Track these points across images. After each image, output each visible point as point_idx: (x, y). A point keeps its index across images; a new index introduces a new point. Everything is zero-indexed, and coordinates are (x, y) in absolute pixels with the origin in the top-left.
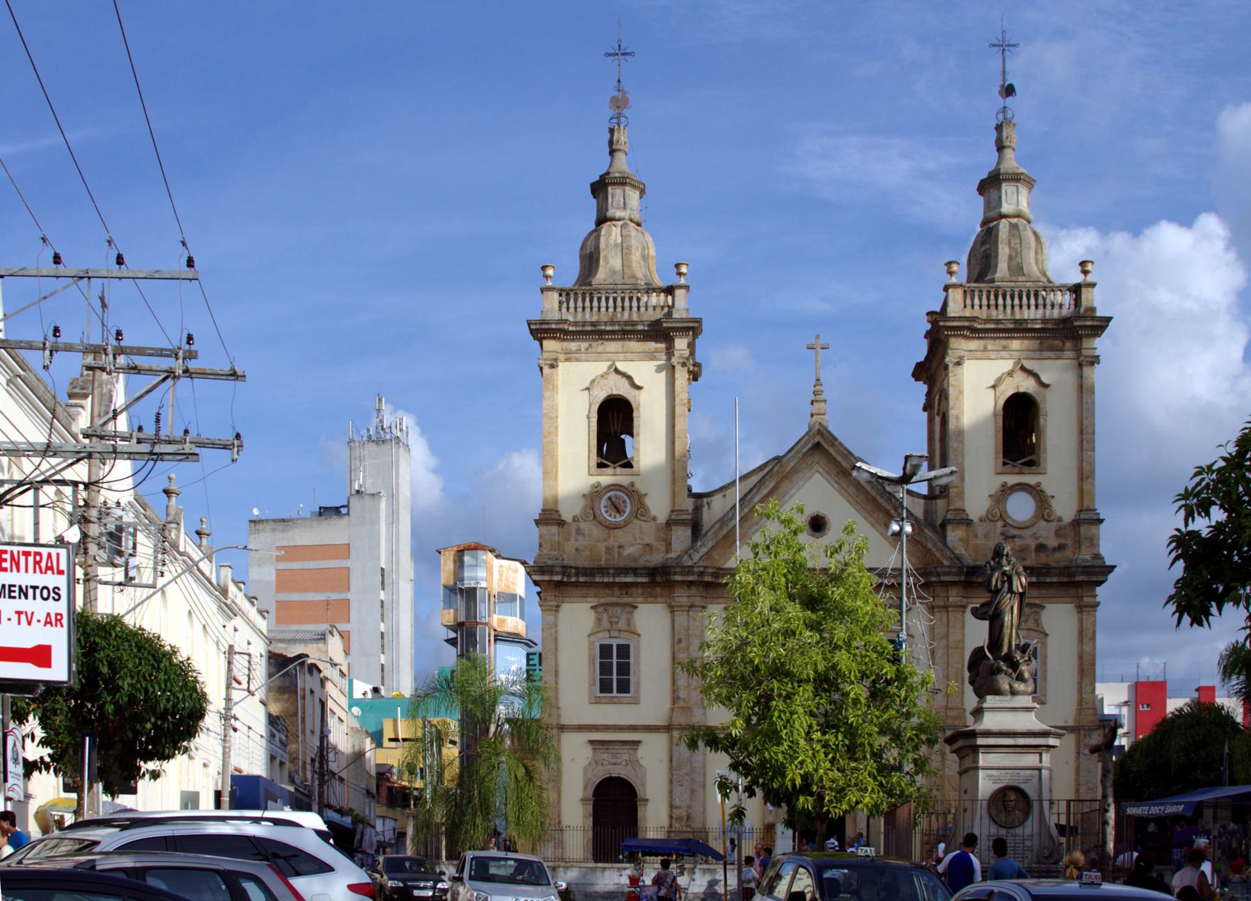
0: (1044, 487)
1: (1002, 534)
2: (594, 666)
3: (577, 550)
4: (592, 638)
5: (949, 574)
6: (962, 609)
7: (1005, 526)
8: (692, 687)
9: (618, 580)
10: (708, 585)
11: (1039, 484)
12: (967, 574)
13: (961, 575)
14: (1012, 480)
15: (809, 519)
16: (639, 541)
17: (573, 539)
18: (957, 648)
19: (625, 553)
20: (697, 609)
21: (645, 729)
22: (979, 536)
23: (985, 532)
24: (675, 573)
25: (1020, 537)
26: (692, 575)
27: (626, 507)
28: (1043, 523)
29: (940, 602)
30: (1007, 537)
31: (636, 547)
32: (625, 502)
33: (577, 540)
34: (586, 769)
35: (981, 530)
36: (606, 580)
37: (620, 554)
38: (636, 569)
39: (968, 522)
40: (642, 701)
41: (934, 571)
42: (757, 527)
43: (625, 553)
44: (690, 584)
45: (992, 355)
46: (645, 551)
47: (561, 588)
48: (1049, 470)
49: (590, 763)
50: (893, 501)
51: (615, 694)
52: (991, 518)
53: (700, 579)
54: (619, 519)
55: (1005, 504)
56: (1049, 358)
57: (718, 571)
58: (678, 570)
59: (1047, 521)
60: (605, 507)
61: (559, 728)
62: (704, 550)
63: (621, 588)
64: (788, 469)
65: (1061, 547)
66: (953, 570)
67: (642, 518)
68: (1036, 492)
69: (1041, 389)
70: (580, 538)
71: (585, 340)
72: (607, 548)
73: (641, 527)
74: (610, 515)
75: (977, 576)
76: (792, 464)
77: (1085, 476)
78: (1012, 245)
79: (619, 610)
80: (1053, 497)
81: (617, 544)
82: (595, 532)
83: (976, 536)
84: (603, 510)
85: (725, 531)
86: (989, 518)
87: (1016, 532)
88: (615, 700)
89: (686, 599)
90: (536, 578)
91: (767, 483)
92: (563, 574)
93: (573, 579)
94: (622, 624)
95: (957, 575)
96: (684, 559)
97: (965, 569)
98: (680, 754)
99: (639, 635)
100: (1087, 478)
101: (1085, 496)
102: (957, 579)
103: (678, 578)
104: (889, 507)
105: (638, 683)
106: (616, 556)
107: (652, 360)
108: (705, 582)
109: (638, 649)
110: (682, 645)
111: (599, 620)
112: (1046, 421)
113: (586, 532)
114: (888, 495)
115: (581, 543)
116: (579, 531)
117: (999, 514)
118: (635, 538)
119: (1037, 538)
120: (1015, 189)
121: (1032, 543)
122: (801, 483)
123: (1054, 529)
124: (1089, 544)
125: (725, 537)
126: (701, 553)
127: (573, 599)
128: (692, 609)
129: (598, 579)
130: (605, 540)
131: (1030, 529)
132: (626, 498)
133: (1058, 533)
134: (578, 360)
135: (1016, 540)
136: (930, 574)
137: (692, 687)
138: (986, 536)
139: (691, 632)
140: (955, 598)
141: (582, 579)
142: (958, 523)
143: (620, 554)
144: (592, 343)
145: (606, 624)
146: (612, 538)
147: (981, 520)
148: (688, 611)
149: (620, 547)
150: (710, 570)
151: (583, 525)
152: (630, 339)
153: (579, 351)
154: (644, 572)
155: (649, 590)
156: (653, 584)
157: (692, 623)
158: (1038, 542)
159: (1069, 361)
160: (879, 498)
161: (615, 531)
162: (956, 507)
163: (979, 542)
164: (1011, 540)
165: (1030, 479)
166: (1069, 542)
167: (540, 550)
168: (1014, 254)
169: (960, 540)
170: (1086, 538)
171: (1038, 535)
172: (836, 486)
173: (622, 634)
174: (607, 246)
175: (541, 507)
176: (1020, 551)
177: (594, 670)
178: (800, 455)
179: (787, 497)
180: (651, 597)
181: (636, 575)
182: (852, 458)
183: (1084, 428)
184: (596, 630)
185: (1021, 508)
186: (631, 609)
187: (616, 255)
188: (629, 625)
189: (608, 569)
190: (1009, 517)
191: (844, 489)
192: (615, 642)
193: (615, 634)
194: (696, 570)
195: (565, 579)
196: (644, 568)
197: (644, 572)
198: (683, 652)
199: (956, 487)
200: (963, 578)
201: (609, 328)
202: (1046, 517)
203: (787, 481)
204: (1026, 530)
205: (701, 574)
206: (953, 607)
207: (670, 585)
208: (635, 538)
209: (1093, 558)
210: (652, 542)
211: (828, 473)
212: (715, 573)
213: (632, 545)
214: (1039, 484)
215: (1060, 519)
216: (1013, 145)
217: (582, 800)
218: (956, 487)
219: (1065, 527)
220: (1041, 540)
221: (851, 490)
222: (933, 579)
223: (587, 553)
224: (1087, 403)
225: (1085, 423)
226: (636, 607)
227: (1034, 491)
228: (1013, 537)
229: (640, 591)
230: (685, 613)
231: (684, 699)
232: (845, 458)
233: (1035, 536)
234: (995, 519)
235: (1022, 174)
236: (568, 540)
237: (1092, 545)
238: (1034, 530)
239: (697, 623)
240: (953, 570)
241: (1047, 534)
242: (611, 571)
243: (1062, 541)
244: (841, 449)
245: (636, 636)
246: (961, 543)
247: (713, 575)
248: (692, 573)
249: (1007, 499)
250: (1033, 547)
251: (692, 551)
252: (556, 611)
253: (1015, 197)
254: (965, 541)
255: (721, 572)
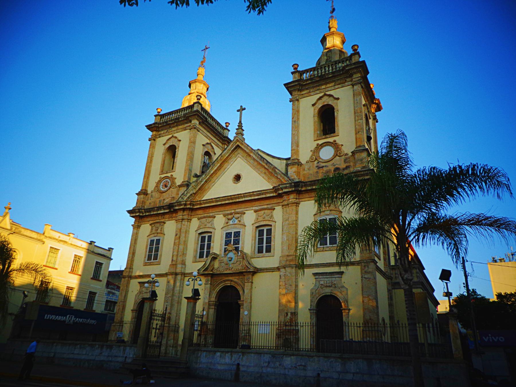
0: (337, 142)
1: (317, 167)
2: (147, 249)
3: (150, 203)
4: (148, 237)
5: (286, 188)
6: (296, 205)
7: (318, 163)
8: (179, 255)
9: (159, 212)
10: (192, 210)
11: (335, 141)
12: (295, 186)
13: (292, 188)
14: (320, 142)
15: (234, 176)
16: (170, 196)
17: (149, 199)
18: (293, 224)
19: (165, 202)
20: (185, 220)
21: (159, 276)
22: (306, 169)
23: (308, 167)
24: (176, 206)
25: (326, 166)
26: (182, 205)
27: (168, 184)
28: (337, 158)
29: (285, 203)
30: (319, 168)
31: (169, 199)
32: (169, 182)
33: (150, 200)
34: (136, 296)
35: (306, 167)
36: (155, 213)
37: (163, 202)
38: (163, 206)
39: (299, 164)
40: (162, 263)
41: (279, 188)
42: (214, 184)
43: (165, 202)
44: (184, 210)
45: (312, 94)
46: (172, 200)
47: (143, 219)
48: (340, 134)
49: (138, 293)
50: (265, 161)
51: (152, 261)
52: (311, 160)
53: (185, 207)
54: (166, 189)
55: (319, 153)
56: (339, 88)
57: (192, 202)
58: (176, 204)
59: (339, 156)
60: (162, 185)
61: (128, 277)
62: (189, 195)
63: (162, 216)
64: (225, 157)
65: (347, 167)
66: (287, 185)
67: (173, 187)
68: (334, 145)
69: (335, 101)
70: (152, 199)
71: (165, 129)
72: (160, 201)
73: (172, 191)
74: (163, 188)
75: (302, 187)
76: (227, 155)
77: (357, 132)
78: (328, 55)
79: (158, 225)
80: (342, 145)
81: (163, 199)
82: (156, 195)
83: (304, 170)
84: (161, 187)
85: (199, 187)
86: (311, 161)
87: (324, 164)
88: (152, 264)
89: (181, 217)
90: (132, 215)
91: (216, 164)
92: (139, 212)
93: (144, 214)
94: (159, 231)
95: (290, 188)
96: (180, 200)
97: (293, 184)
98: (169, 287)
99: (164, 235)
100: (358, 132)
101: (358, 141)
102: (290, 190)
103: (177, 208)
104: (264, 164)
105: (161, 255)
106: (162, 203)
107: (185, 130)
108: (189, 208)
109: (163, 241)
110: (178, 236)
111: (152, 229)
112: (338, 113)
113: (154, 196)
114: (263, 159)
115: (152, 200)
116: (152, 196)
117: (315, 158)
118: (169, 195)
119: (334, 166)
120: (332, 38)
121: (332, 168)
122: (232, 163)
123: (343, 159)
124: (360, 163)
125: (199, 189)
126: (187, 197)
127: (146, 223)
128: (183, 221)
129: (152, 213)
130: (159, 198)
131: (331, 162)
132: (169, 181)
133: (345, 161)
134: (163, 136)
135: (324, 168)
136: (278, 189)
137: (179, 255)
138: (309, 169)
139: (182, 231)
140: (292, 200)
141: (147, 214)
142: (293, 165)
143: (163, 202)
144: (168, 130)
145: (154, 231)
146: (162, 197)
147: (307, 162)
148: (182, 222)
149: (164, 200)
150: (188, 203)
151: (153, 194)
152: (179, 125)
153: (164, 133)
154: (166, 207)
155: (171, 215)
156: (170, 212)
157: (183, 227)
158: (335, 167)
159: (349, 86)
160: (260, 162)
161: (163, 194)
162: (294, 158)
163: (305, 172)
164: (321, 168)
165: (331, 140)
166: (352, 164)
167: (136, 205)
168: (328, 58)
169: (294, 172)
170: (359, 160)
171: (335, 164)
172: (245, 161)
173: (159, 235)
174: (184, 101)
175: (141, 189)
176: (326, 173)
177: (147, 251)
178: (230, 151)
179: (226, 170)
180: (170, 219)
181: (164, 209)
182: (249, 147)
183: (356, 111)
184: (150, 234)
185: (327, 153)
186: (163, 224)
187: (187, 102)
188: (161, 231)
189: (154, 208)
190: (320, 158)
191: (248, 161)
192: (155, 238)
193: (156, 235)
194: (182, 203)
195: (141, 214)
196: (166, 206)
197: (166, 207)
198: (177, 240)
199: (294, 150)
200: (293, 189)
201: (171, 122)
202: (338, 154)
203: (227, 163)
204: (329, 163)
205: (185, 205)
206: (291, 204)
207: (176, 211)
208: (169, 195)
209: (361, 169)
210: (175, 196)
211: (243, 156)
212: (190, 203)
213: (168, 198)
214: (335, 141)
215: (346, 154)
216: (335, 26)
217: (132, 310)
218: (294, 150)
219: (349, 158)
220: (337, 166)
221: (252, 161)
222: (280, 192)
223: (153, 204)
224: (357, 100)
225: (356, 109)
226: (165, 223)
227: (333, 145)
228: (323, 167)
229: (168, 216)
230: (181, 222)
231: (175, 261)
232: (247, 148)
233: (333, 165)
234: (313, 160)
235: (334, 31)
236: (148, 200)
237: (362, 163)
238: (333, 161)
239: (185, 227)
240: (287, 185)
241: (340, 163)
242: (156, 209)
243: (347, 164)
244: (245, 145)
245: (163, 235)
246: (294, 174)
247: (190, 204)
248: (181, 205)
249: (319, 151)
250: (333, 170)
251: (183, 196)
252: (138, 228)
253: (332, 41)
254: (298, 173)
255: (195, 203)
